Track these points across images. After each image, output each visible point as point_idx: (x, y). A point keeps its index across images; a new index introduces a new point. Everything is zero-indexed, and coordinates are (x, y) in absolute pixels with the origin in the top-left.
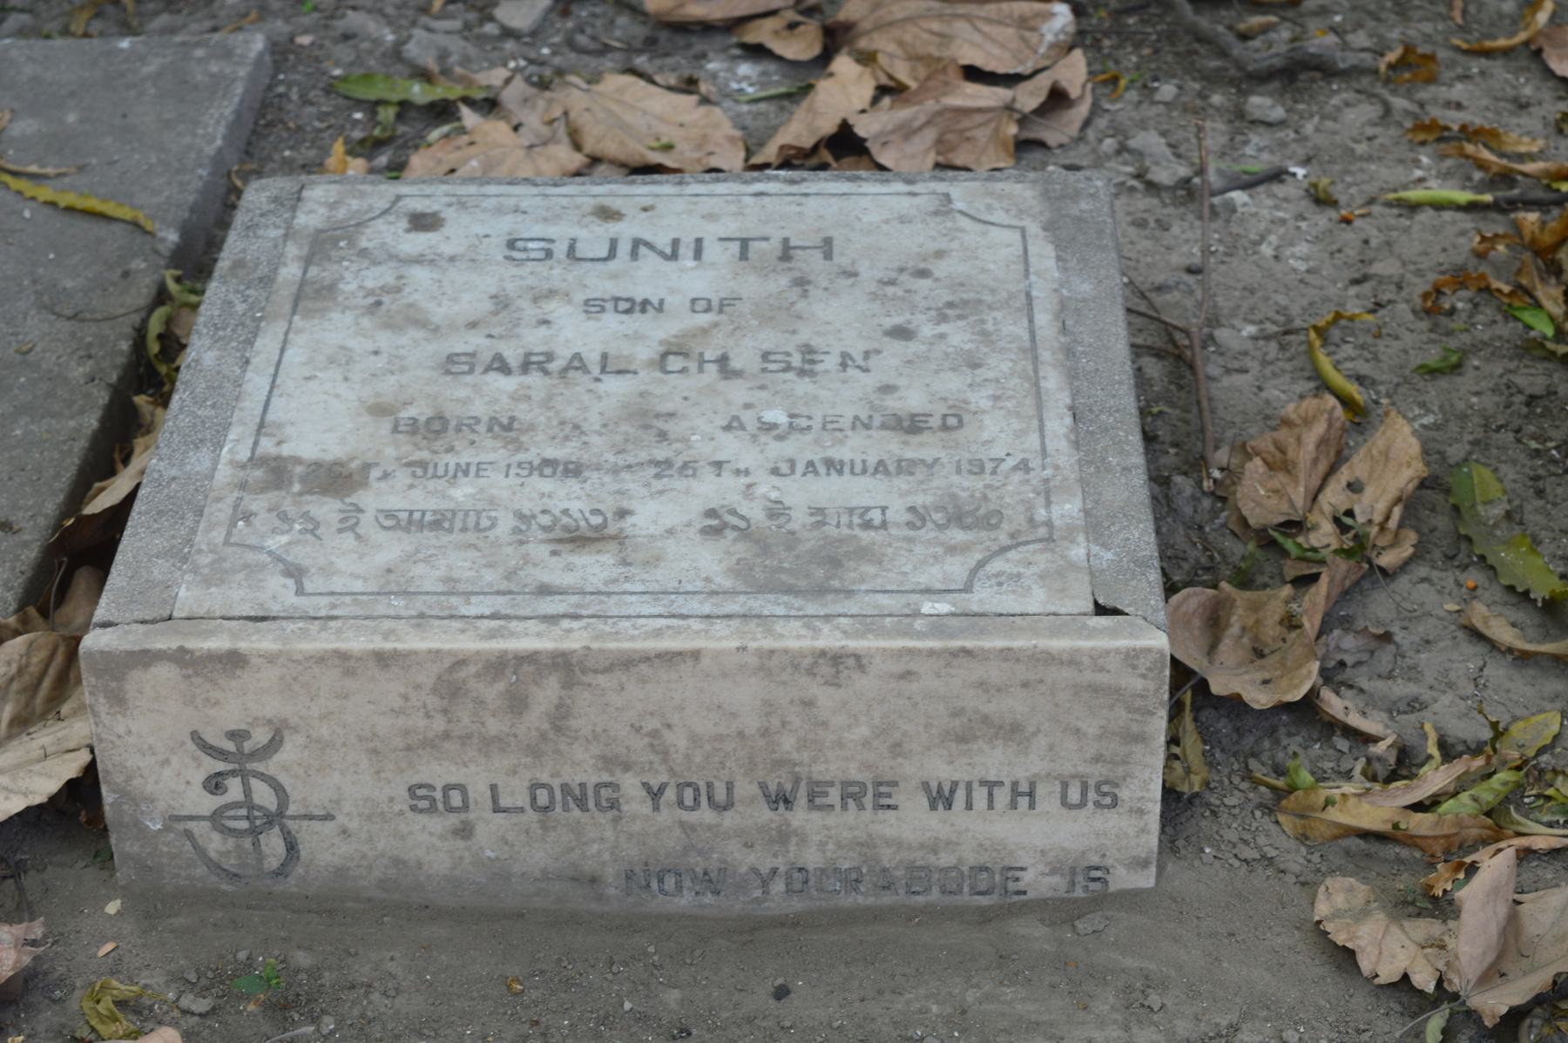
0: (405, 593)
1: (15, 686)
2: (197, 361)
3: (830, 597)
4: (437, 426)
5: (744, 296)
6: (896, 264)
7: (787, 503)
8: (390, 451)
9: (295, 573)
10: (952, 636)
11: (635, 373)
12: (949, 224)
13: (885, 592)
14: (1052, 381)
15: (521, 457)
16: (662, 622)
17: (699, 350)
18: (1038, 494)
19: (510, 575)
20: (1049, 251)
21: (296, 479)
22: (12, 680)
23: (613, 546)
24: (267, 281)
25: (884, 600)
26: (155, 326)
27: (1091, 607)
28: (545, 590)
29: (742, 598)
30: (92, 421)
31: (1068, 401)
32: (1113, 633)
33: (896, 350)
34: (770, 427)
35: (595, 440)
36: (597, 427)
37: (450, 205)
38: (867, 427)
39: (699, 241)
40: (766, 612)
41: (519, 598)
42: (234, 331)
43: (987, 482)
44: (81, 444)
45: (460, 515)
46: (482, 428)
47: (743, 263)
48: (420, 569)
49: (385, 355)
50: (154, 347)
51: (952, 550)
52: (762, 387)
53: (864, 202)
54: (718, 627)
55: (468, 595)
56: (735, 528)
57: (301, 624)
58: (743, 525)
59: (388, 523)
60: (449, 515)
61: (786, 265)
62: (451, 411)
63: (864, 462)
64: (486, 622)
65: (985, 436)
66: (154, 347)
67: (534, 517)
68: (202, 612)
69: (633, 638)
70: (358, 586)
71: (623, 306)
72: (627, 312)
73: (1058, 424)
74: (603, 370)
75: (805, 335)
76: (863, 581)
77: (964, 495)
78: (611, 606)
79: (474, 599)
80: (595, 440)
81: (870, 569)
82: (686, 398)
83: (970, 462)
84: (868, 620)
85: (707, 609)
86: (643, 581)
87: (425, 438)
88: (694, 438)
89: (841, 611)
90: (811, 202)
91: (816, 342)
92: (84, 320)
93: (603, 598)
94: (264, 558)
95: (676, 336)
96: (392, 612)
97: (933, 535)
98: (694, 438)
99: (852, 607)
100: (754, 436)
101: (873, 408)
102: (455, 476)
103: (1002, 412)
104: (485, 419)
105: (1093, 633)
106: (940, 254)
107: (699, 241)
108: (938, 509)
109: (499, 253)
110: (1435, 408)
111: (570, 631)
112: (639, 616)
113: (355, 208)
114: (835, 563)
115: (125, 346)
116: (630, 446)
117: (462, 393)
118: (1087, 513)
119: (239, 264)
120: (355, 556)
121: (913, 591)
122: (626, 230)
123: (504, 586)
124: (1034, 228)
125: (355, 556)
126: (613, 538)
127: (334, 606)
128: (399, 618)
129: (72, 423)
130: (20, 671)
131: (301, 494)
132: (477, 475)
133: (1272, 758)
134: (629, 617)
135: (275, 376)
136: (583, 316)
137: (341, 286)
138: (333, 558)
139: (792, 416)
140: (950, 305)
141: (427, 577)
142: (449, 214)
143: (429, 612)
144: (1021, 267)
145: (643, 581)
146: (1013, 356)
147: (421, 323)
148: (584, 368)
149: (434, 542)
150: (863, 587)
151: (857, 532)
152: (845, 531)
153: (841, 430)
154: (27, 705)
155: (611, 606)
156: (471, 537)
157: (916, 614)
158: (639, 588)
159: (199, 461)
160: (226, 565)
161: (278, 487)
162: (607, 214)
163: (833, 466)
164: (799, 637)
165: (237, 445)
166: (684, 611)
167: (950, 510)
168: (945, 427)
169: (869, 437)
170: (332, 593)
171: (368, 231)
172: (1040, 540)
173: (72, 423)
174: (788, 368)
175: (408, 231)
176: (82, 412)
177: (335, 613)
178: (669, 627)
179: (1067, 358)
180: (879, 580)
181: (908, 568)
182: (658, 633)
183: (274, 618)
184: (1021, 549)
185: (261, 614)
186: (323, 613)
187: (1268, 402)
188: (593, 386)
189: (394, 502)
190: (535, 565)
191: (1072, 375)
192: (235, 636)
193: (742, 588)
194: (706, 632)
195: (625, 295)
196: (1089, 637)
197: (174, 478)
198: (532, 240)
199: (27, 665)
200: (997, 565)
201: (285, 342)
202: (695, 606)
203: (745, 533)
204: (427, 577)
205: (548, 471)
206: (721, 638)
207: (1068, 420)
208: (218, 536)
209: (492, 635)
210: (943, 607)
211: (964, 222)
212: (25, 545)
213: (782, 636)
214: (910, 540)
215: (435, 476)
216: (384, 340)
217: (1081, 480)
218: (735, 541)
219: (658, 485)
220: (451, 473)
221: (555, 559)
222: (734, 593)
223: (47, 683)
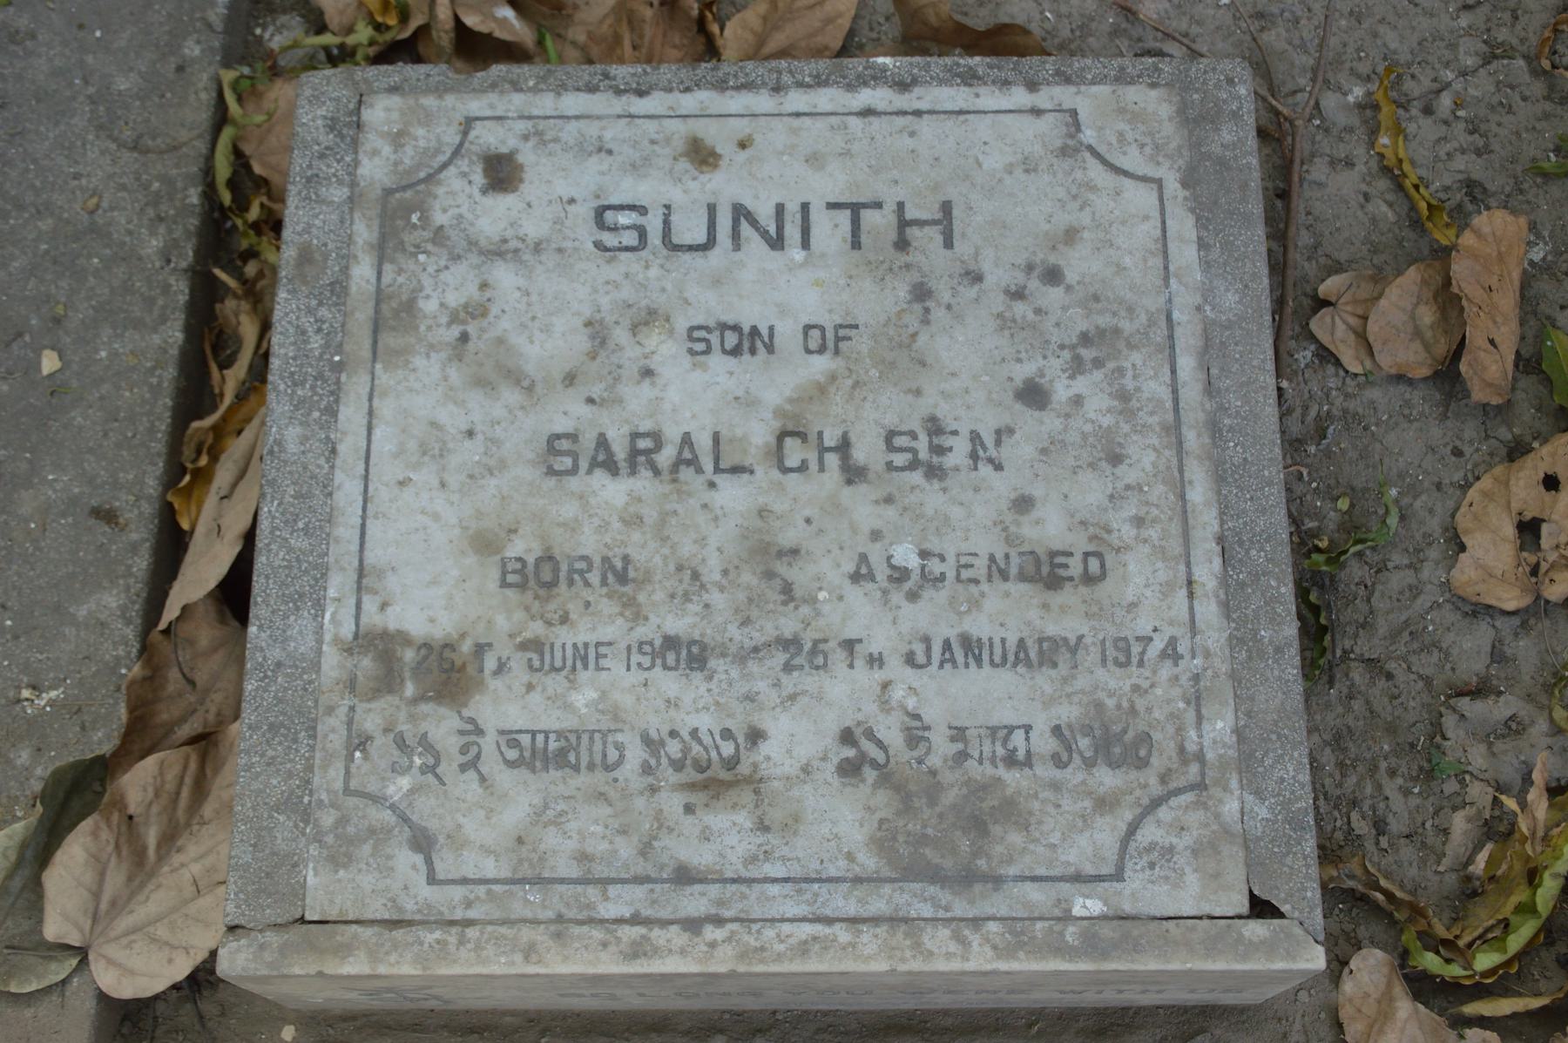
0: (538, 881)
1: (155, 809)
2: (278, 443)
3: (978, 888)
4: (547, 576)
5: (861, 321)
6: (1021, 260)
7: (927, 719)
8: (502, 623)
9: (423, 843)
10: (1104, 955)
11: (752, 472)
12: (1079, 175)
13: (1034, 879)
14: (1199, 493)
15: (643, 632)
16: (808, 929)
17: (816, 430)
18: (1188, 703)
19: (645, 850)
20: (1190, 221)
21: (407, 674)
22: (150, 804)
23: (747, 796)
24: (339, 289)
25: (1035, 894)
26: (223, 170)
27: (1244, 908)
28: (684, 876)
29: (887, 889)
30: (174, 334)
31: (1216, 528)
32: (1268, 947)
33: (1033, 426)
34: (899, 575)
35: (716, 598)
36: (717, 577)
37: (526, 138)
38: (1005, 576)
39: (805, 207)
40: (913, 914)
41: (658, 887)
42: (313, 388)
43: (1134, 680)
44: (170, 373)
45: (585, 738)
46: (594, 578)
47: (856, 253)
48: (551, 839)
49: (480, 437)
50: (226, 197)
51: (1105, 804)
52: (889, 500)
53: (983, 125)
54: (865, 938)
55: (605, 882)
56: (874, 764)
57: (437, 935)
58: (881, 758)
59: (512, 754)
60: (573, 739)
61: (903, 258)
62: (563, 546)
63: (1003, 641)
64: (627, 928)
65: (1130, 596)
66: (226, 197)
67: (662, 743)
68: (333, 914)
69: (779, 957)
70: (490, 868)
71: (731, 340)
72: (735, 352)
73: (1207, 571)
74: (717, 470)
75: (931, 402)
76: (1010, 860)
77: (1110, 703)
78: (753, 902)
79: (613, 890)
80: (716, 598)
81: (1016, 838)
82: (808, 521)
83: (1117, 640)
84: (1019, 925)
85: (852, 909)
86: (784, 859)
87: (537, 597)
88: (822, 595)
89: (990, 911)
90: (926, 126)
91: (944, 411)
92: (147, 151)
93: (744, 888)
94: (387, 816)
95: (791, 401)
96: (529, 914)
97: (1080, 776)
98: (822, 595)
99: (998, 904)
100: (885, 592)
101: (1009, 540)
102: (574, 669)
103: (1147, 549)
104: (597, 560)
105: (1252, 948)
106: (1071, 235)
107: (805, 207)
108: (1087, 730)
109: (585, 233)
110: (1546, 234)
111: (713, 945)
112: (783, 920)
113: (422, 143)
114: (979, 826)
115: (194, 197)
116: (755, 613)
117: (569, 510)
118: (1237, 731)
119: (306, 257)
120: (482, 813)
121: (1061, 879)
122: (725, 185)
123: (640, 867)
124: (1172, 185)
125: (482, 813)
126: (748, 780)
127: (469, 904)
128: (535, 922)
129: (157, 339)
130: (157, 795)
131: (415, 701)
132: (598, 668)
133: (1374, 808)
134: (773, 920)
135: (366, 478)
136: (687, 361)
137: (421, 303)
138: (461, 820)
139: (924, 554)
140: (1085, 339)
141: (560, 853)
142: (526, 156)
143: (571, 914)
144: (1157, 262)
145: (784, 859)
146: (1155, 441)
147: (515, 377)
148: (694, 463)
149: (561, 789)
150: (1012, 871)
151: (1001, 771)
152: (989, 770)
153: (976, 582)
154: (170, 820)
155: (753, 902)
156: (600, 777)
157: (1067, 918)
158: (777, 871)
159: (301, 625)
160: (351, 830)
161: (391, 691)
162: (702, 156)
163: (972, 649)
164: (949, 956)
165: (339, 621)
166: (828, 912)
167: (1098, 733)
168: (1088, 579)
169: (1007, 594)
170: (464, 881)
171: (441, 191)
172: (1192, 787)
173: (157, 339)
174: (913, 465)
175: (484, 192)
176: (163, 319)
177: (472, 914)
178: (815, 938)
179: (1214, 445)
180: (1027, 859)
181: (1055, 838)
182: (803, 949)
183: (410, 923)
184: (1174, 802)
185: (395, 917)
186: (459, 914)
187: (1374, 220)
188: (708, 496)
189: (515, 717)
190: (671, 830)
191: (1220, 477)
192: (374, 957)
193: (886, 872)
194: (853, 945)
195: (730, 319)
196: (1245, 957)
197: (279, 665)
198: (621, 208)
199: (163, 782)
200: (1149, 833)
201: (371, 413)
202: (843, 902)
203: (886, 776)
204: (560, 853)
205: (671, 658)
206: (870, 957)
207: (1217, 562)
208: (336, 774)
209: (637, 951)
210: (1095, 907)
211: (1096, 171)
212: (134, 548)
213: (931, 953)
214: (1056, 786)
215: (554, 669)
216: (478, 408)
217: (1233, 676)
218: (876, 786)
219: (790, 683)
220: (569, 663)
221: (690, 819)
222: (876, 880)
223: (185, 793)
